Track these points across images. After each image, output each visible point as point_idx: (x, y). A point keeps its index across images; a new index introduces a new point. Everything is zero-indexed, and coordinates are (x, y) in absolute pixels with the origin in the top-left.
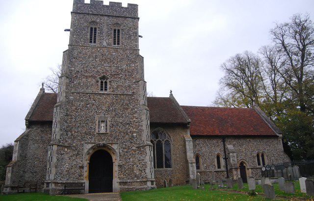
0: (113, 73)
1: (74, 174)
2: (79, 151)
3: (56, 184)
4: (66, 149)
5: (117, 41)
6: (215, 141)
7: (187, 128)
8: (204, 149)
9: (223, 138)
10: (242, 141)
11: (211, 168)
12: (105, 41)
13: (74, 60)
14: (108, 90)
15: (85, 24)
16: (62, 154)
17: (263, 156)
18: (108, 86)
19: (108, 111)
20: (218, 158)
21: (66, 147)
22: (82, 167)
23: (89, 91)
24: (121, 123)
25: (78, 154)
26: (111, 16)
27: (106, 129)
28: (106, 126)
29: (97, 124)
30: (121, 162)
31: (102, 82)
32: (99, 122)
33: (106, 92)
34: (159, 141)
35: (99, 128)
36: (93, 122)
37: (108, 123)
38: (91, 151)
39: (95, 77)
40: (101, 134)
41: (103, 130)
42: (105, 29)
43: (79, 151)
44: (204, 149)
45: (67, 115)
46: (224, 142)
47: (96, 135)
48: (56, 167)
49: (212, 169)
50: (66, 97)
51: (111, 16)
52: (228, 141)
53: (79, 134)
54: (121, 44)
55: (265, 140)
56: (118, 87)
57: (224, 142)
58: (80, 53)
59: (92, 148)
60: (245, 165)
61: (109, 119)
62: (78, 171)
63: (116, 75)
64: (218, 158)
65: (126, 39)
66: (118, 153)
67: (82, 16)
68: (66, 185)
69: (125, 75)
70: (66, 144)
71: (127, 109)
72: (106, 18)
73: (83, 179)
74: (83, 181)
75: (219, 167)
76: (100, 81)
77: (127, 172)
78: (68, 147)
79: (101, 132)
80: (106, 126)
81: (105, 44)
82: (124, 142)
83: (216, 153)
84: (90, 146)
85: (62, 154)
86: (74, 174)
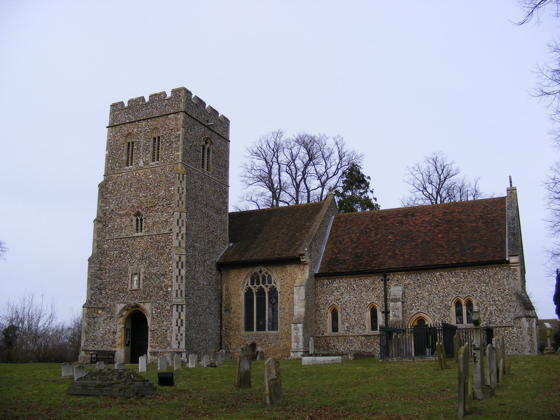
0: (148, 206)
1: (107, 340)
2: (112, 314)
3: (86, 351)
4: (100, 312)
5: (155, 157)
6: (367, 281)
7: (305, 264)
8: (346, 297)
9: (385, 273)
10: (424, 277)
11: (356, 329)
12: (142, 159)
13: (109, 195)
14: (143, 230)
15: (122, 140)
16: (94, 318)
17: (469, 304)
18: (144, 224)
19: (141, 259)
20: (374, 312)
21: (100, 309)
22: (115, 333)
23: (123, 235)
24: (155, 274)
25: (111, 317)
26: (149, 118)
27: (139, 284)
28: (139, 279)
29: (130, 278)
30: (153, 326)
31: (137, 220)
32: (132, 275)
33: (140, 234)
34: (273, 286)
35: (131, 283)
36: (126, 276)
37: (142, 276)
38: (124, 313)
39: (128, 215)
40: (134, 290)
41: (135, 286)
42: (142, 141)
43: (112, 314)
44: (346, 297)
45: (100, 269)
46: (385, 281)
47: (129, 292)
48: (86, 333)
49: (357, 331)
50: (97, 247)
51: (149, 118)
52: (394, 278)
53: (113, 293)
54: (160, 159)
55: (478, 272)
56: (153, 224)
57: (385, 281)
58: (115, 183)
59: (124, 309)
60: (416, 323)
61: (142, 270)
62: (112, 337)
63: (151, 207)
64: (374, 312)
65: (166, 150)
66: (150, 315)
67: (118, 128)
68: (98, 353)
69: (163, 205)
70: (100, 306)
71: (162, 254)
72: (144, 123)
73: (115, 347)
74: (116, 349)
75: (374, 326)
76: (134, 219)
77: (160, 339)
78: (103, 309)
79: (134, 288)
80: (139, 279)
81: (141, 164)
82: (158, 300)
83: (369, 303)
84: (123, 305)
85: (94, 318)
86: (107, 340)
